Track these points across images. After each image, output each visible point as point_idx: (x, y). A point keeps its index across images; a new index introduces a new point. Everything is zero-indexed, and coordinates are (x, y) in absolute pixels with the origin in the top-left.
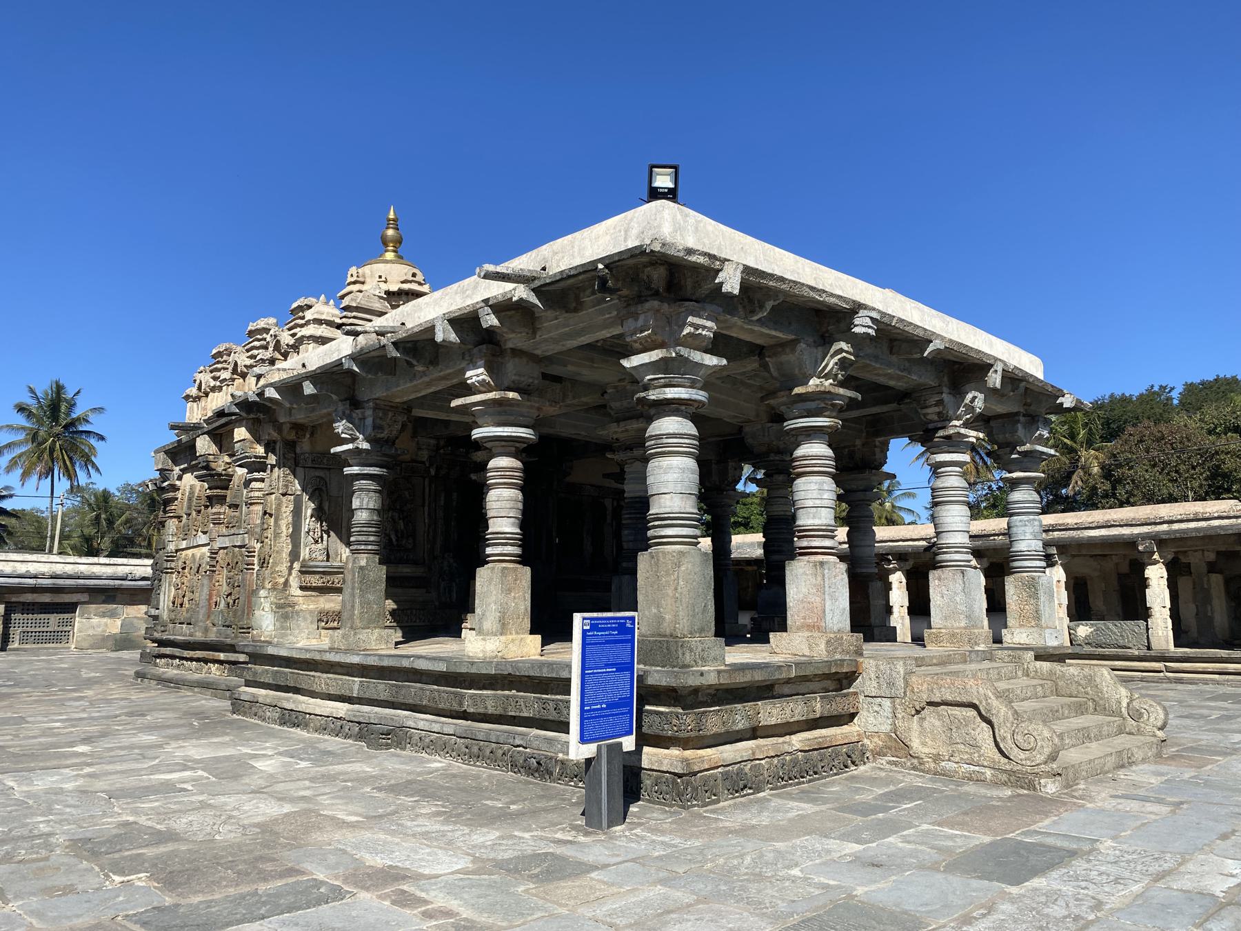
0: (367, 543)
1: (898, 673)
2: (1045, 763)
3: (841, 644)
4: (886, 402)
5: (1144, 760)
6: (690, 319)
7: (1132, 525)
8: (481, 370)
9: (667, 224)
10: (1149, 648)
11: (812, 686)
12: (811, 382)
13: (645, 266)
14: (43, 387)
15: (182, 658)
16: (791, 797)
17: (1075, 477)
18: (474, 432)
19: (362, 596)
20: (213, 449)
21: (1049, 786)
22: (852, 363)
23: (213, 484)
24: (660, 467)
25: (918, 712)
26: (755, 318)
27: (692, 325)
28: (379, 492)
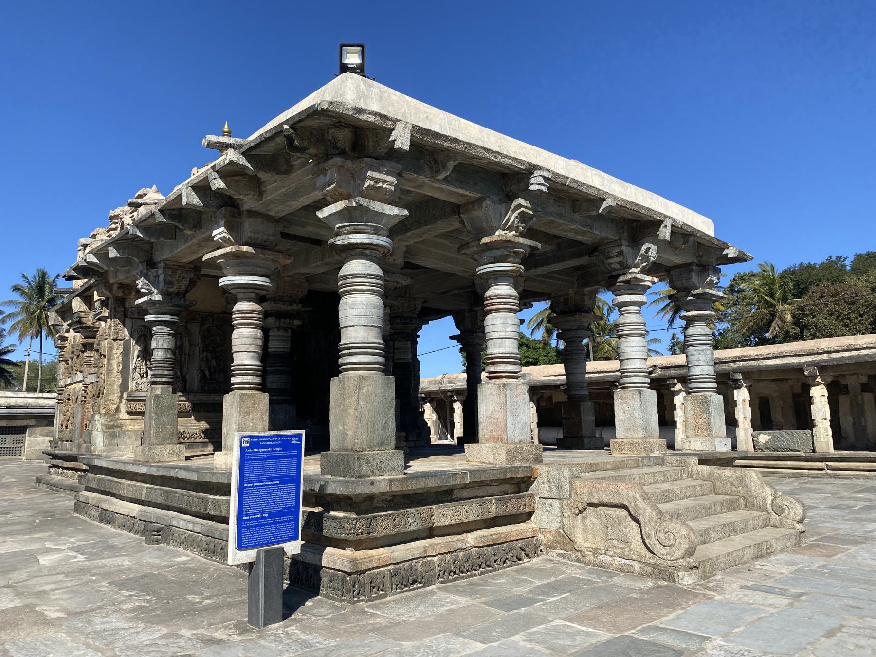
0: (161, 376)
1: (565, 478)
2: (683, 558)
3: (522, 453)
4: (580, 255)
5: (782, 550)
6: (369, 173)
7: (799, 356)
8: (222, 229)
9: (350, 92)
10: (814, 451)
11: (491, 489)
12: (497, 233)
13: (329, 128)
14: (32, 274)
15: (64, 468)
16: (457, 591)
17: (774, 324)
18: (220, 281)
20: (84, 308)
21: (686, 578)
22: (531, 217)
23: (86, 334)
24: (346, 304)
25: (581, 512)
26: (441, 177)
27: (372, 178)
28: (172, 335)
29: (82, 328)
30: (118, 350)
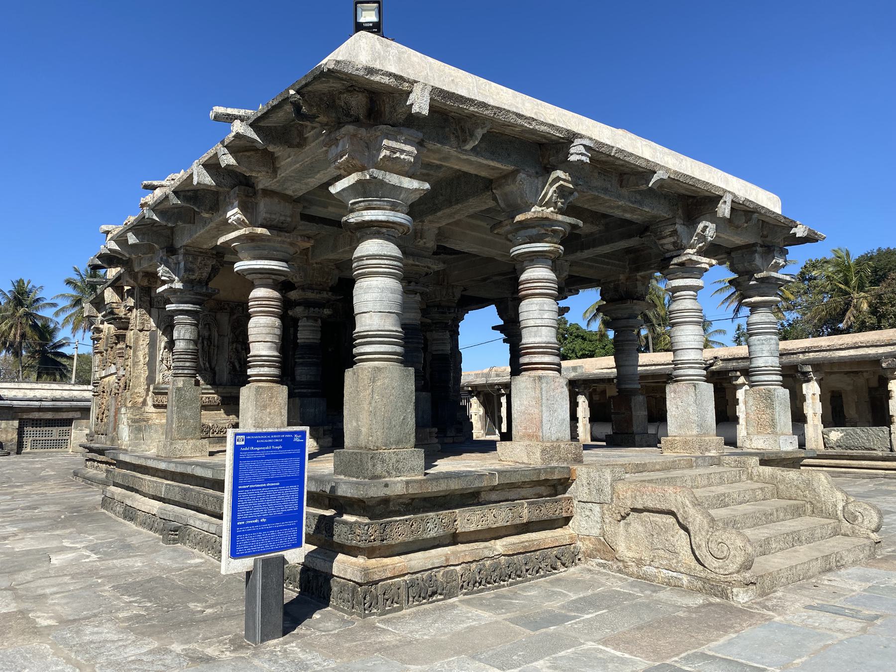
0: (183, 368)
1: (606, 480)
2: (738, 572)
3: (559, 452)
4: (630, 236)
5: (854, 563)
6: (385, 142)
7: (877, 346)
8: (236, 210)
9: (364, 53)
10: (891, 450)
11: (524, 492)
12: (533, 210)
13: (340, 93)
15: (98, 462)
16: (481, 605)
17: (848, 314)
18: (235, 266)
19: (178, 413)
20: (116, 298)
21: (741, 595)
22: (571, 192)
23: (118, 325)
24: (361, 288)
25: (623, 518)
26: (468, 147)
27: (388, 148)
28: (196, 325)
29: (115, 319)
30: (144, 341)
